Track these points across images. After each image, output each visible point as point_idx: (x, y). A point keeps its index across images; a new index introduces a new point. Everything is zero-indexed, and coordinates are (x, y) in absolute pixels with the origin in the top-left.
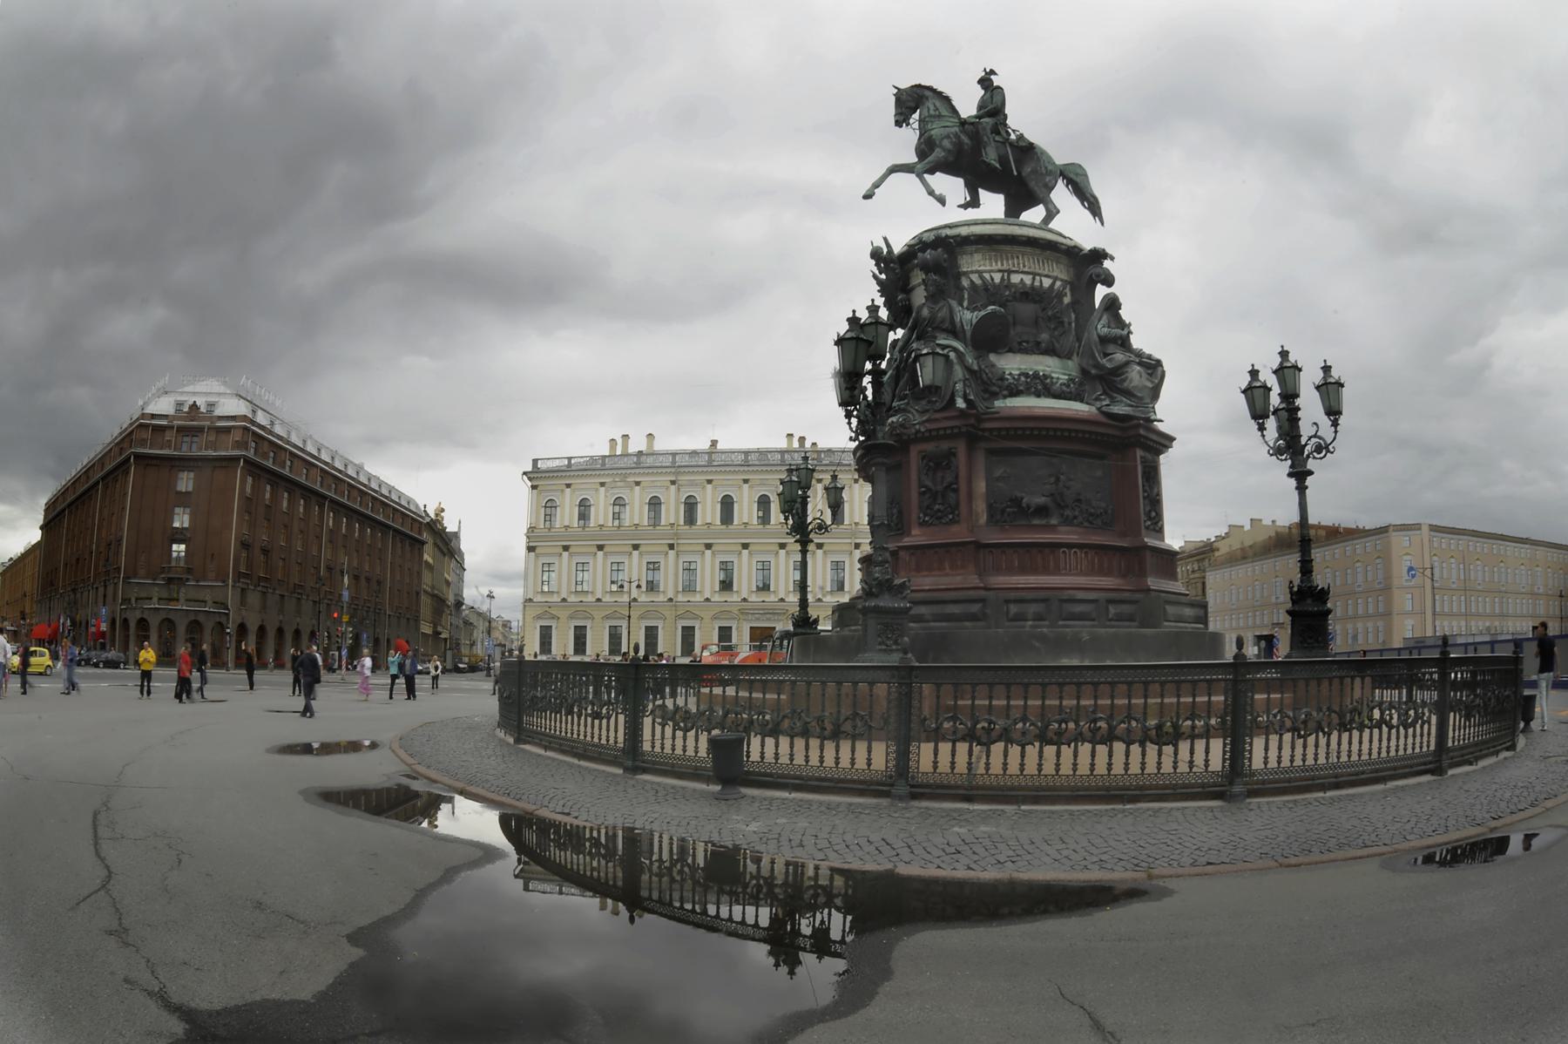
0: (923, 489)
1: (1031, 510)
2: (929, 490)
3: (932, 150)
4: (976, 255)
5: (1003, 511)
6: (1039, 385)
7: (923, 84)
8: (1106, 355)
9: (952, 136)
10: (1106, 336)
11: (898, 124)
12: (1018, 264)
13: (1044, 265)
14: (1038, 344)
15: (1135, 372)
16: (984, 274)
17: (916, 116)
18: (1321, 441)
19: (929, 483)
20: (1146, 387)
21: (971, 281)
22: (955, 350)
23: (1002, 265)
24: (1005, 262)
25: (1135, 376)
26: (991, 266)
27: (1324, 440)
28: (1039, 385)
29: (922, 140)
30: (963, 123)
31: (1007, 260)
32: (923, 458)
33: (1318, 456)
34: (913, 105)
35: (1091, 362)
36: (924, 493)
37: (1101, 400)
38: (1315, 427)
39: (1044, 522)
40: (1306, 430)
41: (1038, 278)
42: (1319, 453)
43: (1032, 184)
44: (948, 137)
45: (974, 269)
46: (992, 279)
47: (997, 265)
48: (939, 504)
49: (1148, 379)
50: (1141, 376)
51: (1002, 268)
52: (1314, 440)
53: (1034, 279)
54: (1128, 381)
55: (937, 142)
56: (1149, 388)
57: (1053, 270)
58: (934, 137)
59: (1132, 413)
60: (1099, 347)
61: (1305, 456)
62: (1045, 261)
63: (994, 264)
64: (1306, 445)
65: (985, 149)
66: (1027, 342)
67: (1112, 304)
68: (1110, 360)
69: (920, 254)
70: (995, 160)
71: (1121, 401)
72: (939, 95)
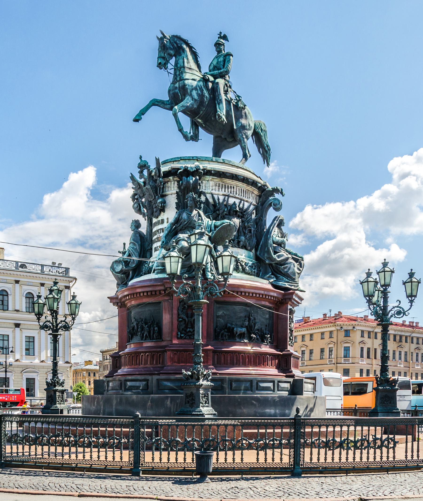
0: (181, 319)
2: (185, 320)
16: (214, 195)
18: (401, 309)
19: (185, 317)
21: (207, 199)
23: (225, 191)
24: (226, 190)
27: (402, 309)
33: (398, 316)
36: (181, 321)
40: (392, 303)
42: (398, 315)
45: (209, 191)
46: (218, 199)
48: (190, 328)
52: (396, 309)
53: (240, 203)
63: (220, 189)
65: (219, 104)
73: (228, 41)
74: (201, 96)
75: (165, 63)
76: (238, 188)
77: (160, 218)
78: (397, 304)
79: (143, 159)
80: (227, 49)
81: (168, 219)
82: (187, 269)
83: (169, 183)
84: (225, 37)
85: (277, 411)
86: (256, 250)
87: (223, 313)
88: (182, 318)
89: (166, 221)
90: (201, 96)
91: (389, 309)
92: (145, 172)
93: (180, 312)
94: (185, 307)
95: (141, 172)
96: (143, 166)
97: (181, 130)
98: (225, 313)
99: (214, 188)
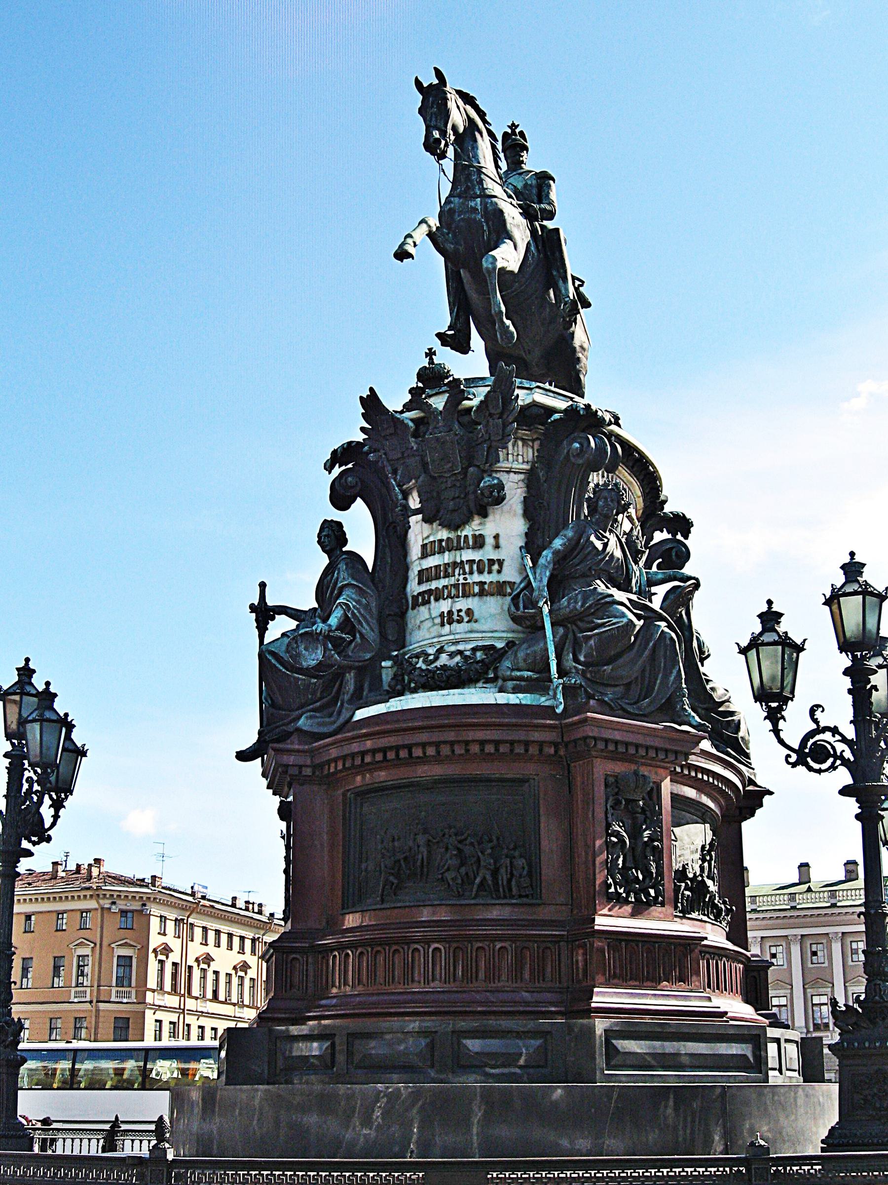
0: (614, 839)
77: (467, 531)
81: (496, 537)
89: (490, 541)
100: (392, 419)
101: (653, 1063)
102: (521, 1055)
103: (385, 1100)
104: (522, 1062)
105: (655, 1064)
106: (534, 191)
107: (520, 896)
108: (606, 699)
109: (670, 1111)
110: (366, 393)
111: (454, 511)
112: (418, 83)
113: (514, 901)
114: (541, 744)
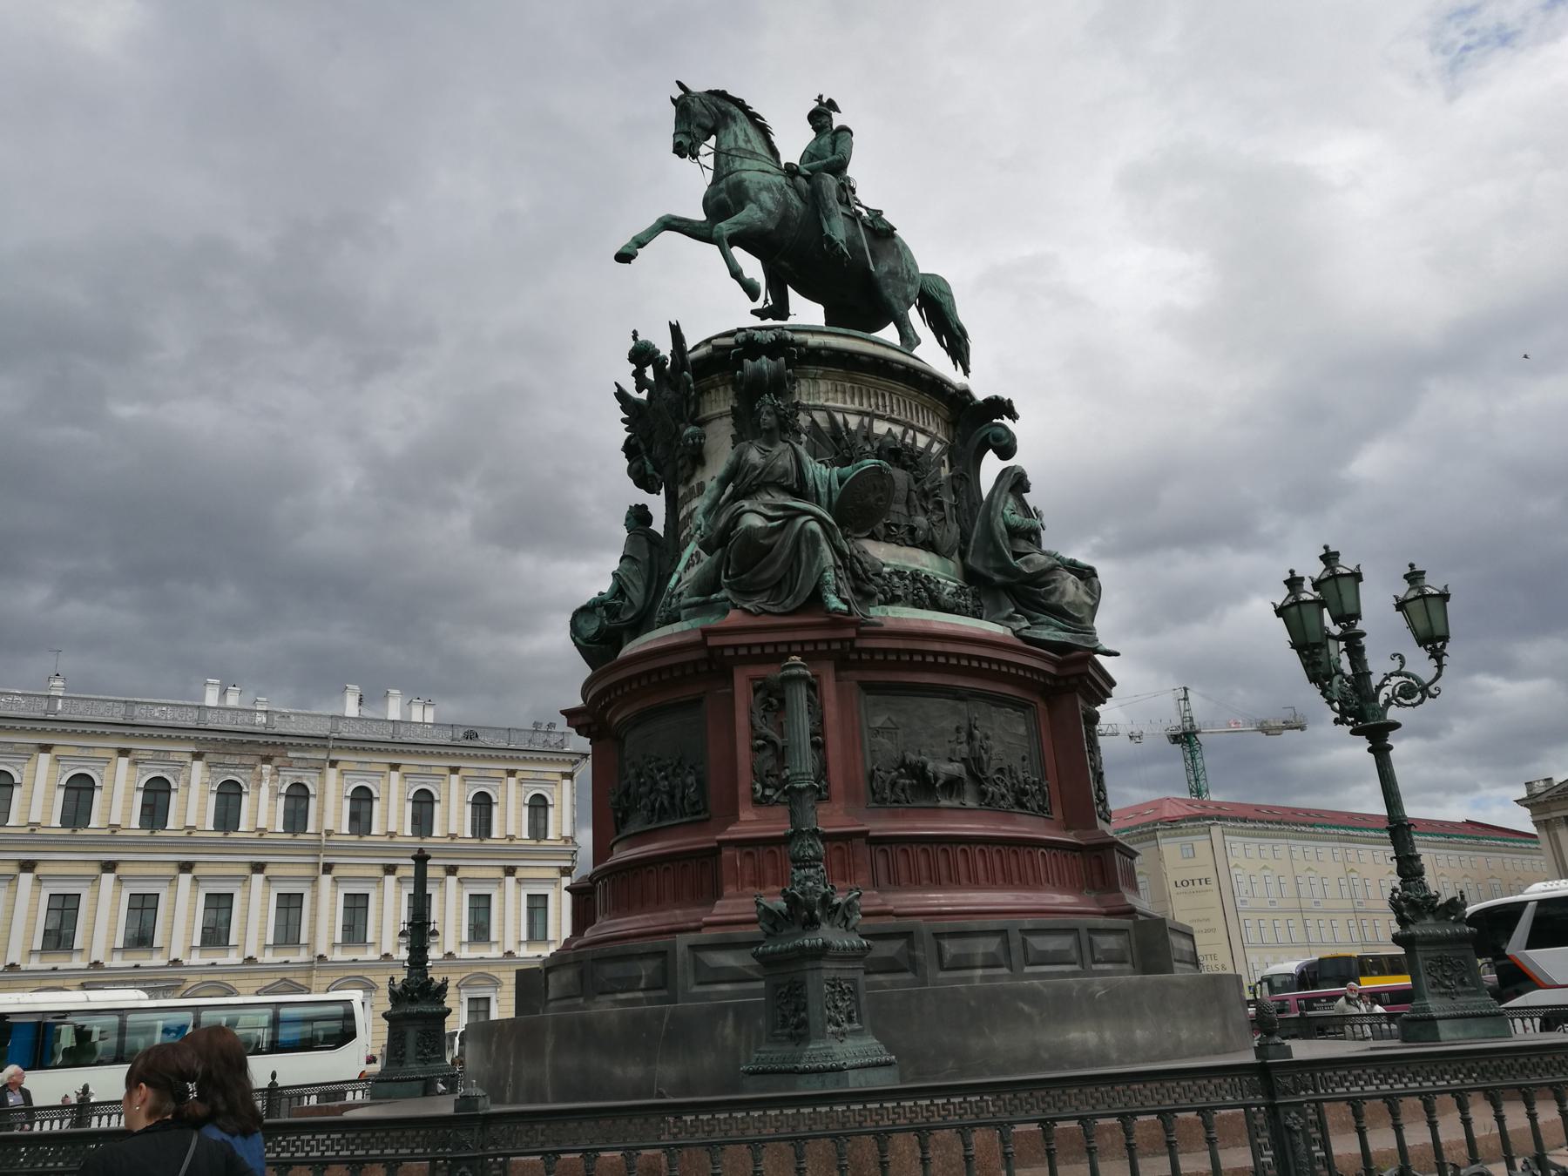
0: (760, 742)
1: (941, 782)
2: (773, 743)
3: (740, 206)
4: (821, 382)
5: (893, 784)
6: (924, 593)
7: (729, 93)
8: (1017, 555)
9: (775, 189)
10: (1017, 527)
11: (680, 150)
12: (885, 406)
13: (917, 413)
14: (912, 530)
15: (1069, 581)
17: (712, 141)
18: (1411, 680)
20: (1086, 603)
22: (819, 519)
24: (865, 401)
25: (1070, 587)
26: (845, 402)
28: (924, 593)
29: (722, 185)
30: (790, 170)
31: (869, 398)
32: (756, 691)
34: (709, 123)
35: (992, 563)
36: (759, 749)
37: (1015, 620)
38: (1397, 661)
39: (956, 803)
40: (1378, 665)
41: (911, 432)
43: (888, 292)
44: (768, 189)
45: (821, 402)
46: (846, 423)
47: (853, 402)
49: (1087, 593)
50: (1077, 588)
51: (861, 408)
52: (1395, 680)
53: (905, 433)
54: (1058, 594)
55: (752, 194)
56: (1089, 605)
57: (929, 424)
58: (747, 183)
59: (1070, 641)
60: (1007, 542)
61: (1381, 701)
62: (920, 408)
64: (1382, 686)
65: (828, 219)
66: (898, 526)
67: (1016, 483)
68: (1026, 563)
69: (748, 362)
70: (842, 241)
71: (1049, 624)
72: (753, 117)
73: (839, 112)
74: (786, 205)
75: (692, 144)
76: (894, 397)
77: (694, 483)
78: (1394, 666)
79: (640, 338)
80: (837, 120)
82: (769, 592)
83: (713, 391)
84: (832, 105)
85: (1108, 1035)
86: (963, 555)
87: (889, 719)
88: (765, 738)
90: (786, 205)
91: (1375, 681)
92: (649, 373)
93: (758, 721)
94: (771, 705)
95: (638, 375)
96: (642, 355)
97: (736, 274)
98: (894, 719)
99: (831, 395)
100: (637, 403)
101: (756, 975)
102: (640, 978)
103: (497, 1034)
104: (642, 985)
105: (760, 977)
106: (829, 148)
107: (693, 814)
108: (746, 606)
109: (729, 1030)
110: (616, 390)
111: (683, 468)
112: (672, 99)
113: (685, 820)
114: (695, 663)
